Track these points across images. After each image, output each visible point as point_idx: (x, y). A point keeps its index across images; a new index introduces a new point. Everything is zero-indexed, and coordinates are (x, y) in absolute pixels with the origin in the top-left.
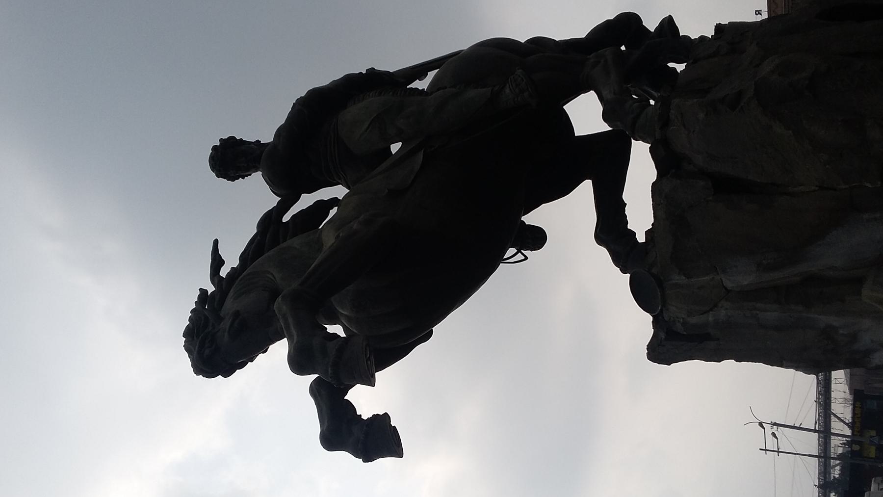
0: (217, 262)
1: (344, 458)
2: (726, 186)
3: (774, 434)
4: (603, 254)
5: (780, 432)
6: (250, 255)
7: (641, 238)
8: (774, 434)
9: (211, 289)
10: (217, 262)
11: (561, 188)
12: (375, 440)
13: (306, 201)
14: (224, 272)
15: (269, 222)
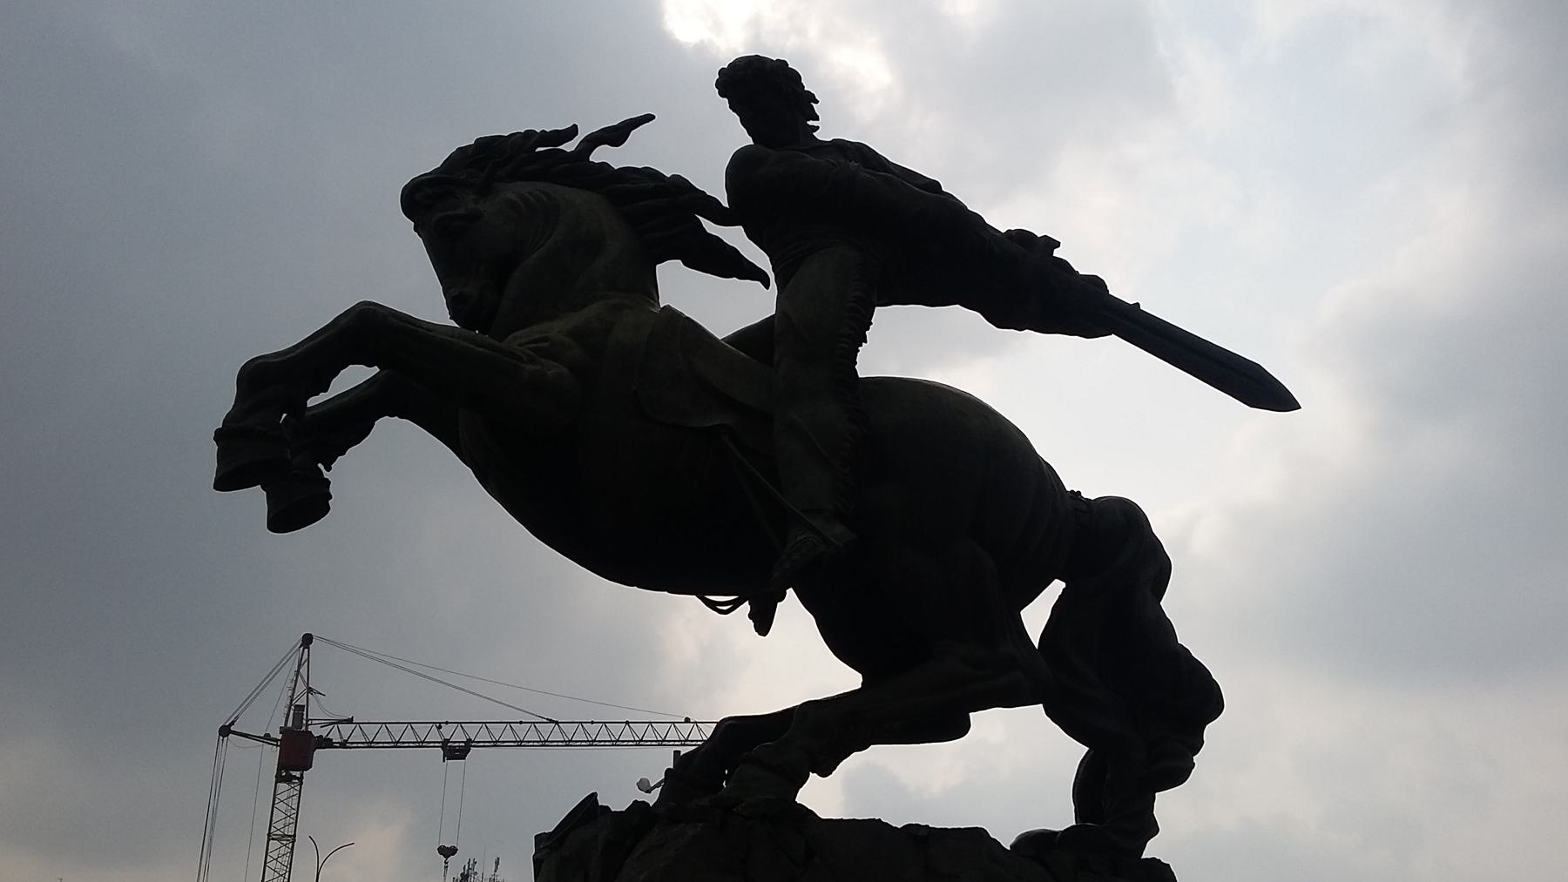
0: (616, 135)
9: (569, 147)
10: (616, 135)
11: (842, 640)
13: (735, 237)
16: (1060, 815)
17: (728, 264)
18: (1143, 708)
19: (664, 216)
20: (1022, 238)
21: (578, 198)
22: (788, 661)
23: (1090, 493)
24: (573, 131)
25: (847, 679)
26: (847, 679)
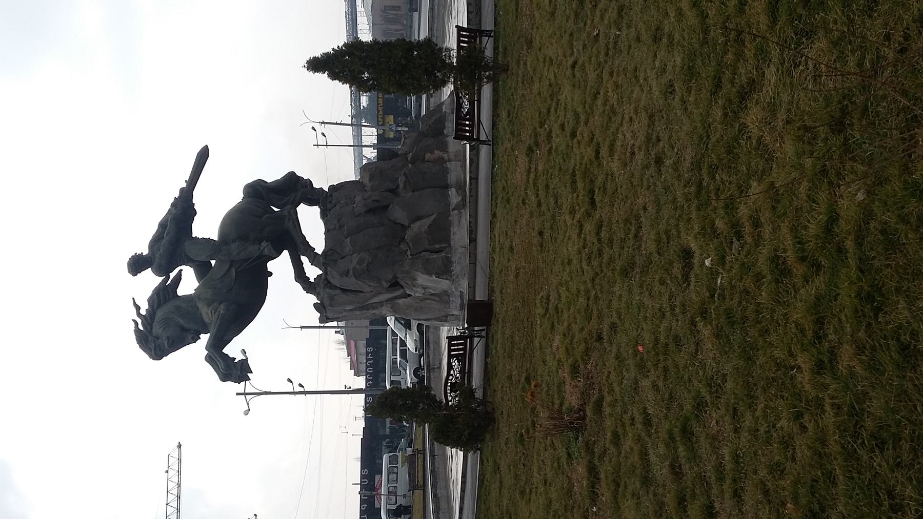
0: (138, 308)
2: (344, 291)
3: (323, 134)
4: (298, 286)
5: (327, 129)
7: (312, 280)
8: (323, 134)
9: (139, 321)
10: (138, 308)
13: (172, 275)
14: (143, 312)
16: (316, 210)
17: (179, 278)
18: (294, 189)
19: (165, 295)
20: (173, 205)
21: (159, 314)
22: (281, 267)
23: (242, 196)
24: (134, 321)
25: (286, 253)
26: (286, 253)
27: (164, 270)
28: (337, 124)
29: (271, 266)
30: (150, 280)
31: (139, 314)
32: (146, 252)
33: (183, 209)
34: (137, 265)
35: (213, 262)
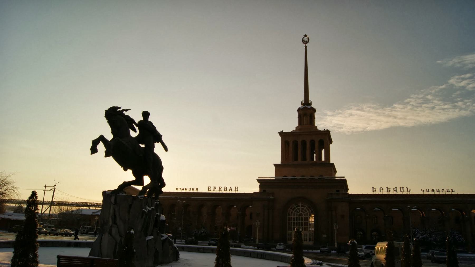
0: (127, 110)
1: (90, 145)
2: (130, 206)
3: (51, 190)
6: (128, 117)
8: (51, 190)
9: (121, 110)
10: (127, 110)
11: (134, 174)
12: (94, 150)
14: (124, 112)
15: (133, 121)
17: (135, 130)
27: (140, 125)
28: (53, 196)
29: (130, 171)
30: (138, 118)
31: (123, 110)
32: (149, 120)
33: (158, 138)
34: (146, 115)
35: (143, 146)
